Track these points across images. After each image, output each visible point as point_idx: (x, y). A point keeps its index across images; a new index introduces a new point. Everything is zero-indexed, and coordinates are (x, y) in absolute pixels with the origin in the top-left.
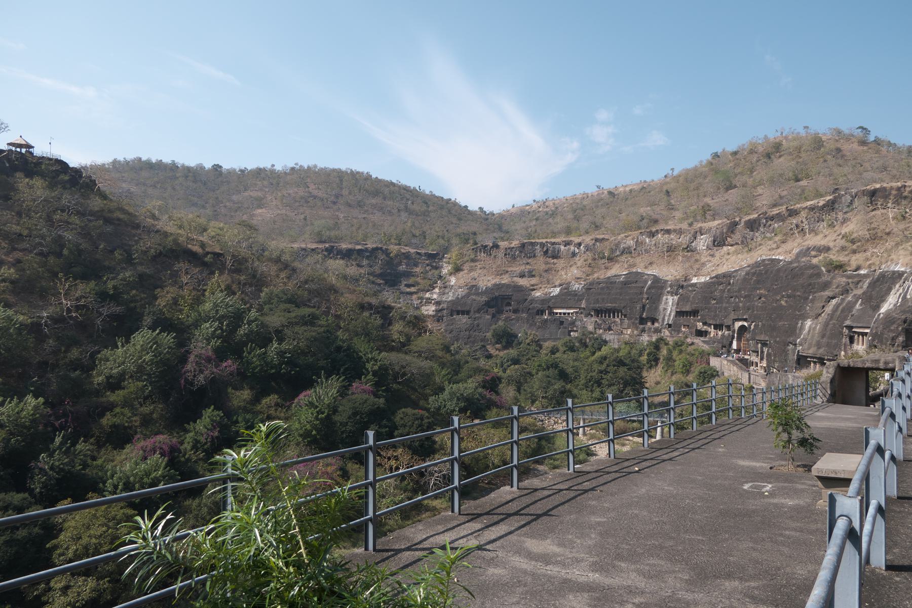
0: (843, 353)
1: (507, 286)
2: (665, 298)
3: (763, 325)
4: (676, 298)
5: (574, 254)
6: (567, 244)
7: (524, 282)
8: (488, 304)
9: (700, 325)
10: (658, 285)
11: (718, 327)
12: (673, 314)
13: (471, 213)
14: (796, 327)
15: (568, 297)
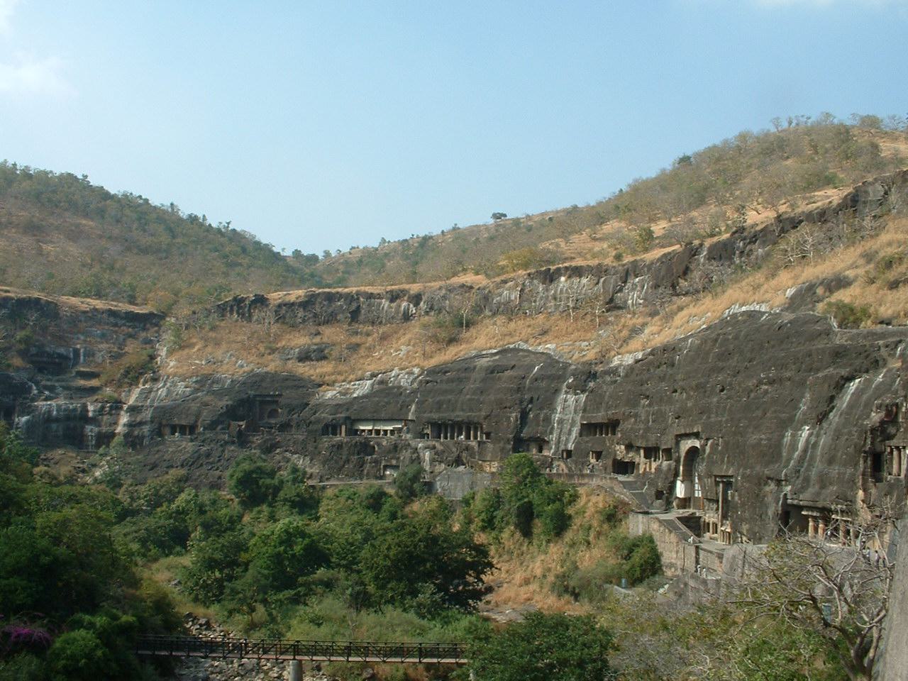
0: (861, 493)
1: (273, 377)
2: (563, 396)
3: (726, 444)
4: (583, 397)
5: (407, 317)
6: (394, 297)
7: (304, 370)
8: (232, 413)
9: (620, 450)
10: (554, 373)
11: (651, 452)
12: (576, 431)
13: (277, 256)
14: (779, 444)
15: (387, 400)
